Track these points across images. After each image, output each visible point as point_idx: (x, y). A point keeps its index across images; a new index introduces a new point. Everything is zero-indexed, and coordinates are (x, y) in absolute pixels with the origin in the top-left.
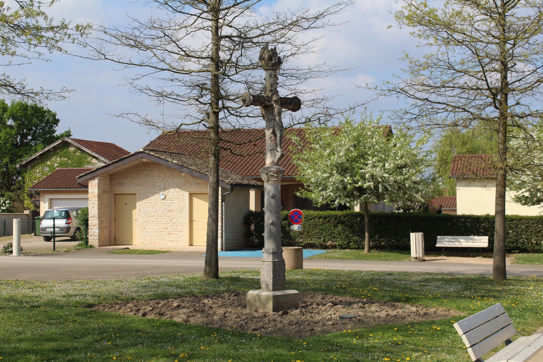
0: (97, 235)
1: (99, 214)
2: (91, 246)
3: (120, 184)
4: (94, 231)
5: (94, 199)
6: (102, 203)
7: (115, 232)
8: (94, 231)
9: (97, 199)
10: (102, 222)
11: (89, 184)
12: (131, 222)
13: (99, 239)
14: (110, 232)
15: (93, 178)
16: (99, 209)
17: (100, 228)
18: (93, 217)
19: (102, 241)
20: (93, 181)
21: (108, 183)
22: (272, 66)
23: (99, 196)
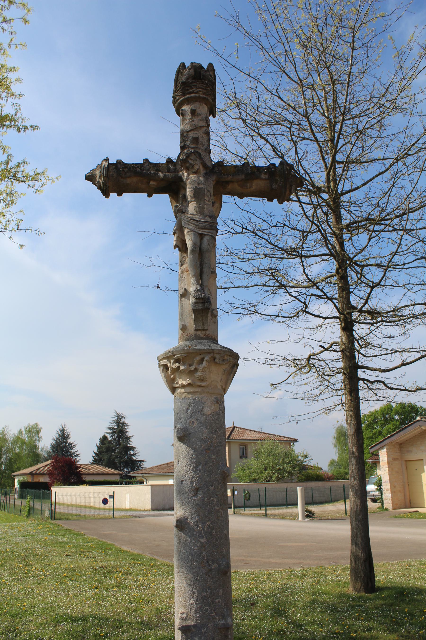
0: (391, 499)
1: (389, 479)
2: (386, 509)
3: (409, 452)
4: (387, 495)
5: (385, 466)
6: (392, 470)
7: (410, 496)
8: (387, 495)
9: (387, 466)
10: (395, 487)
11: (380, 454)
12: (422, 486)
13: (392, 503)
14: (405, 495)
15: (382, 448)
16: (389, 474)
17: (393, 492)
18: (385, 482)
19: (396, 504)
20: (383, 451)
21: (398, 451)
22: (184, 94)
23: (389, 463)
